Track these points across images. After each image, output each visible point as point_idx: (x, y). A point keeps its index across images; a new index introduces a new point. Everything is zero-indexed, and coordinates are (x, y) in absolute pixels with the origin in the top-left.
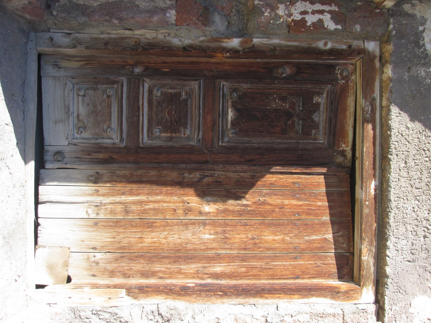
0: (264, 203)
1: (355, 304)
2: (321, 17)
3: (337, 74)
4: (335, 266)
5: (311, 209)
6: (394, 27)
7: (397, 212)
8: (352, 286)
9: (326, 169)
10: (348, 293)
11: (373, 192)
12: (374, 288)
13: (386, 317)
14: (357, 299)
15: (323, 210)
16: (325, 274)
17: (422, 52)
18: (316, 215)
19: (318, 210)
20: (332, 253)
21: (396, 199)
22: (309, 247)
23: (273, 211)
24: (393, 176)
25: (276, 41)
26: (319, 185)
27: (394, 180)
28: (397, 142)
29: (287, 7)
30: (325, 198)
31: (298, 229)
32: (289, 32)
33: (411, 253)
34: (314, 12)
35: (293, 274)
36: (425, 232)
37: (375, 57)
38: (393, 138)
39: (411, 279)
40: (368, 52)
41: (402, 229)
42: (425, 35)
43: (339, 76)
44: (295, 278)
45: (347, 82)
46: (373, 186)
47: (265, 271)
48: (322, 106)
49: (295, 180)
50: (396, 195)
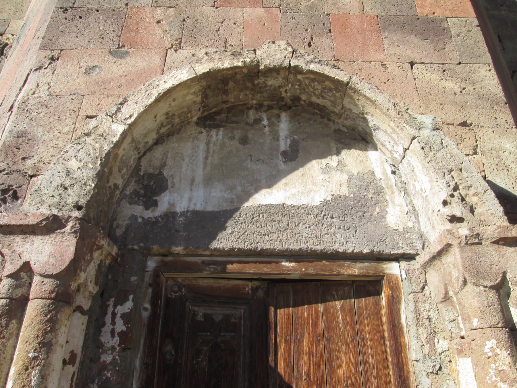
0: (308, 374)
1: (402, 280)
2: (119, 315)
3: (175, 296)
4: (367, 298)
5: (312, 323)
6: (136, 244)
7: (311, 243)
8: (384, 283)
9: (271, 307)
10: (392, 287)
11: (292, 264)
12: (384, 262)
13: (411, 252)
14: (397, 278)
15: (312, 310)
16: (376, 309)
17: (163, 219)
18: (317, 317)
19: (312, 315)
20: (355, 302)
21: (299, 244)
22: (351, 325)
23: (316, 364)
24: (277, 246)
25: (138, 363)
26: (287, 315)
27: (281, 245)
28: (245, 243)
29: (105, 352)
30: (300, 308)
31: (333, 336)
32: (130, 349)
33: (348, 229)
34: (113, 323)
35: (380, 342)
36: (328, 218)
37: (162, 261)
38: (242, 246)
39: (372, 230)
40: (157, 267)
41: (327, 238)
42: (146, 217)
43: (178, 294)
44: (384, 340)
45: (184, 286)
46: (287, 264)
47: (380, 373)
48: (207, 312)
49: (283, 340)
50: (295, 244)
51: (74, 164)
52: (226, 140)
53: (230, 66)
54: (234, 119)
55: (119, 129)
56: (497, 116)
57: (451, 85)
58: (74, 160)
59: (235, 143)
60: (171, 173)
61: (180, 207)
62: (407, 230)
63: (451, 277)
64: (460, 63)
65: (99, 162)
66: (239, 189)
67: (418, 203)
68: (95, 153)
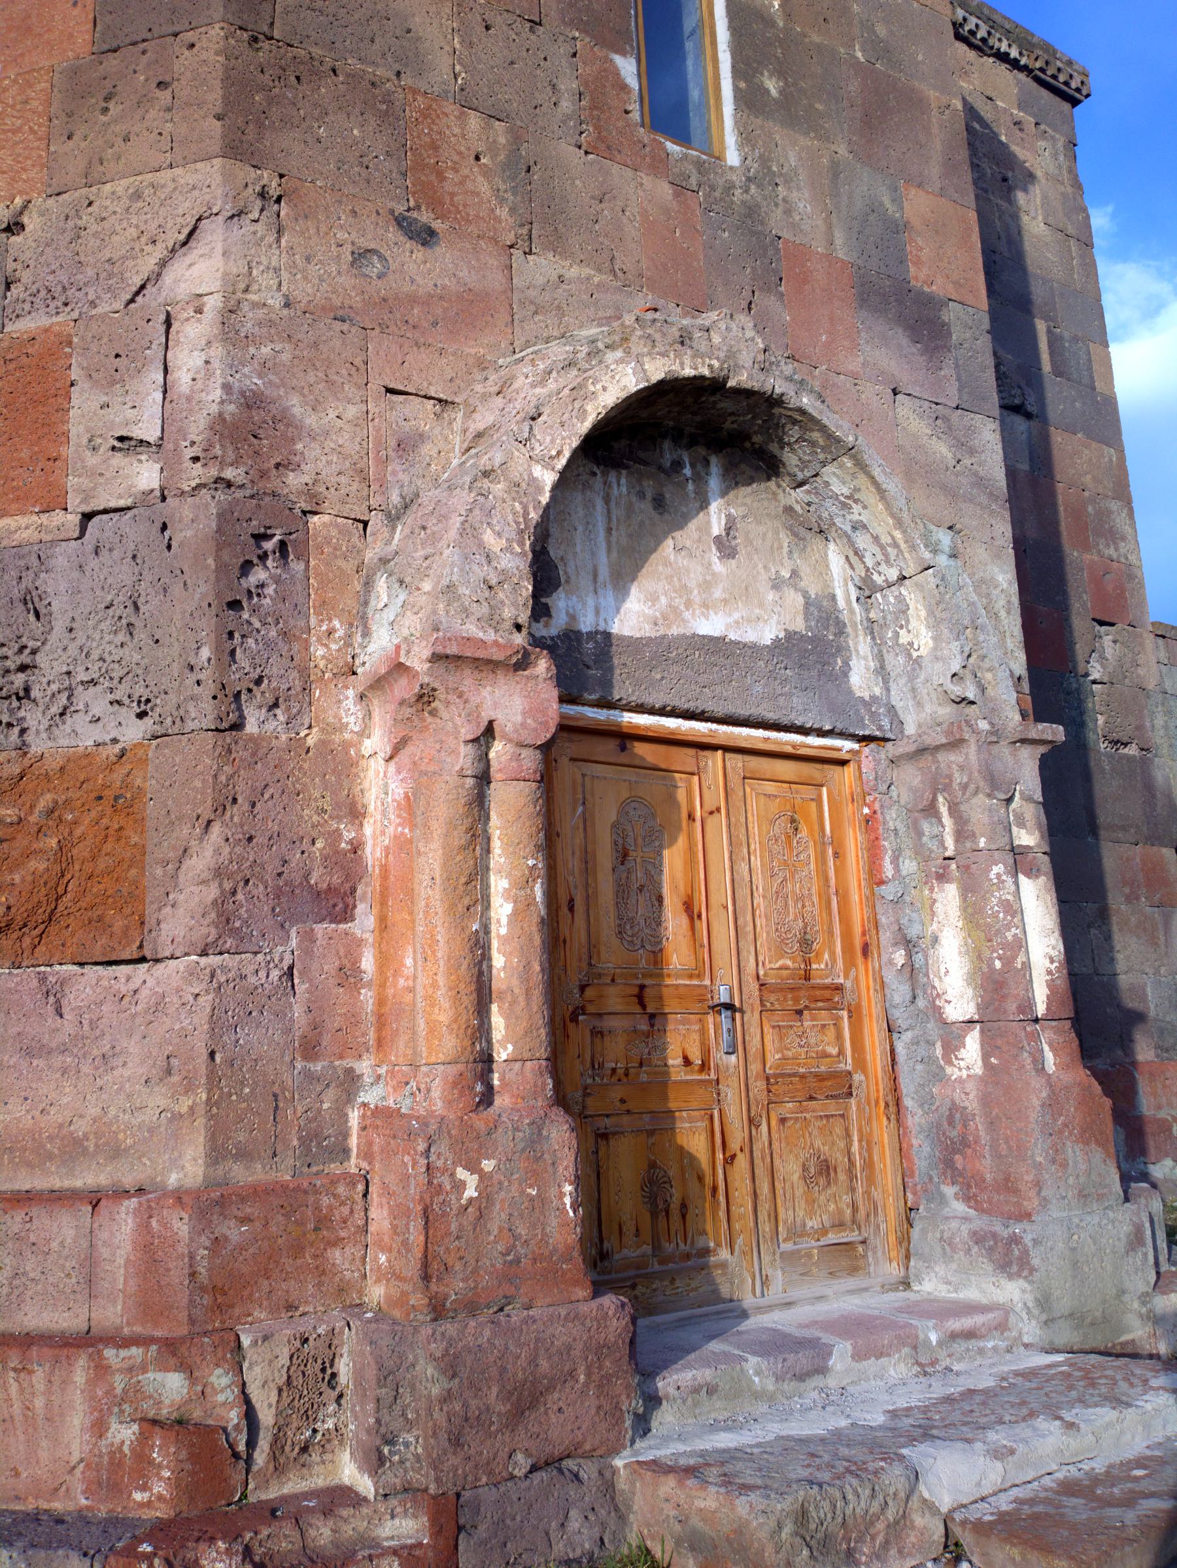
51: (493, 541)
52: (634, 499)
53: (692, 373)
54: (641, 454)
55: (549, 478)
56: (993, 522)
57: (943, 450)
58: (489, 531)
59: (646, 506)
60: (561, 553)
61: (585, 622)
62: (874, 698)
63: (951, 781)
64: (957, 408)
65: (528, 543)
66: (663, 600)
67: (897, 663)
68: (517, 523)
